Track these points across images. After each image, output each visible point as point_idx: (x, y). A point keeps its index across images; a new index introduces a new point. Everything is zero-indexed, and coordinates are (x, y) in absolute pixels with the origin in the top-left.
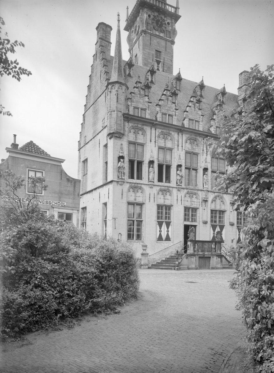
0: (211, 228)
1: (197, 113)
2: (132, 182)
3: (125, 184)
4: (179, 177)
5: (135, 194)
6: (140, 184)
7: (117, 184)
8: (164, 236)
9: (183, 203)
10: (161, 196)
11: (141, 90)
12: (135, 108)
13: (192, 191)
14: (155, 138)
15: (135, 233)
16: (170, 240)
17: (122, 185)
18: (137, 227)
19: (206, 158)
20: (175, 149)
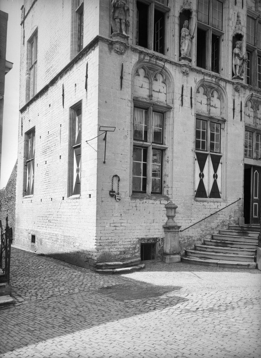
4: (238, 61)
5: (151, 83)
7: (111, 49)
8: (209, 186)
9: (243, 119)
16: (219, 197)
18: (152, 163)
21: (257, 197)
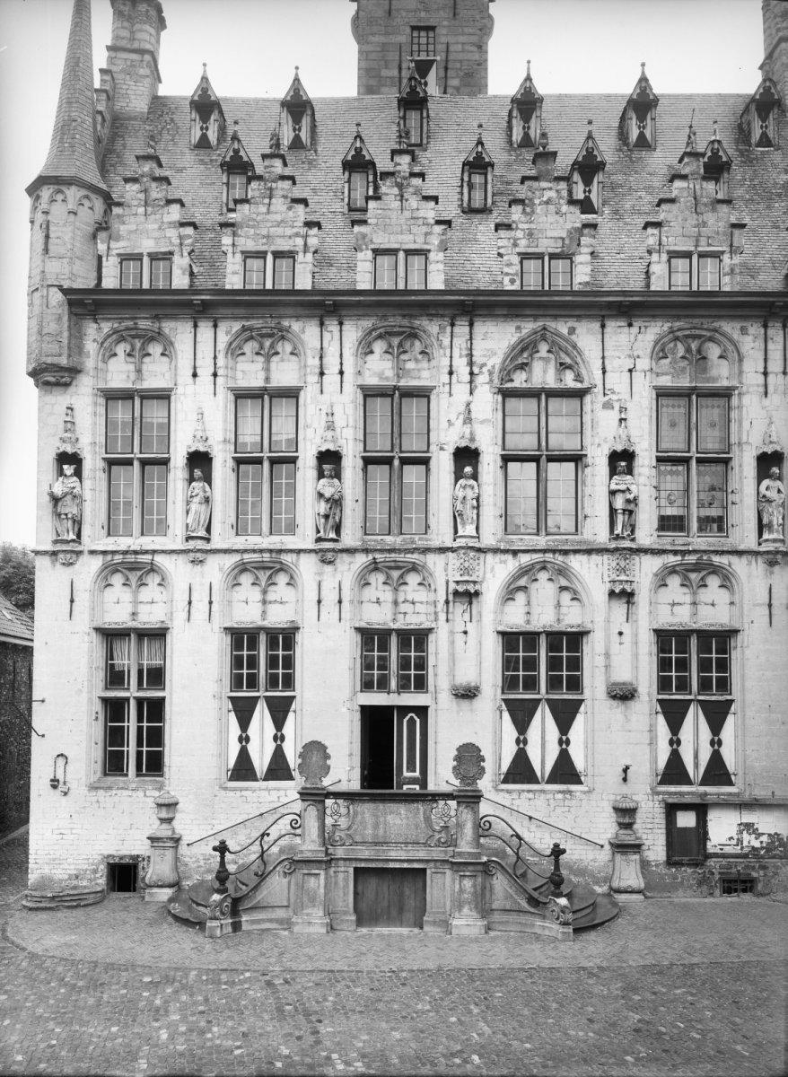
0: (506, 715)
1: (413, 218)
2: (110, 548)
3: (85, 558)
5: (136, 593)
6: (146, 552)
7: (53, 563)
8: (262, 759)
10: (248, 591)
11: (154, 185)
12: (125, 258)
13: (393, 555)
14: (215, 357)
15: (131, 748)
17: (71, 564)
19: (468, 405)
20: (309, 388)
21: (415, 771)
